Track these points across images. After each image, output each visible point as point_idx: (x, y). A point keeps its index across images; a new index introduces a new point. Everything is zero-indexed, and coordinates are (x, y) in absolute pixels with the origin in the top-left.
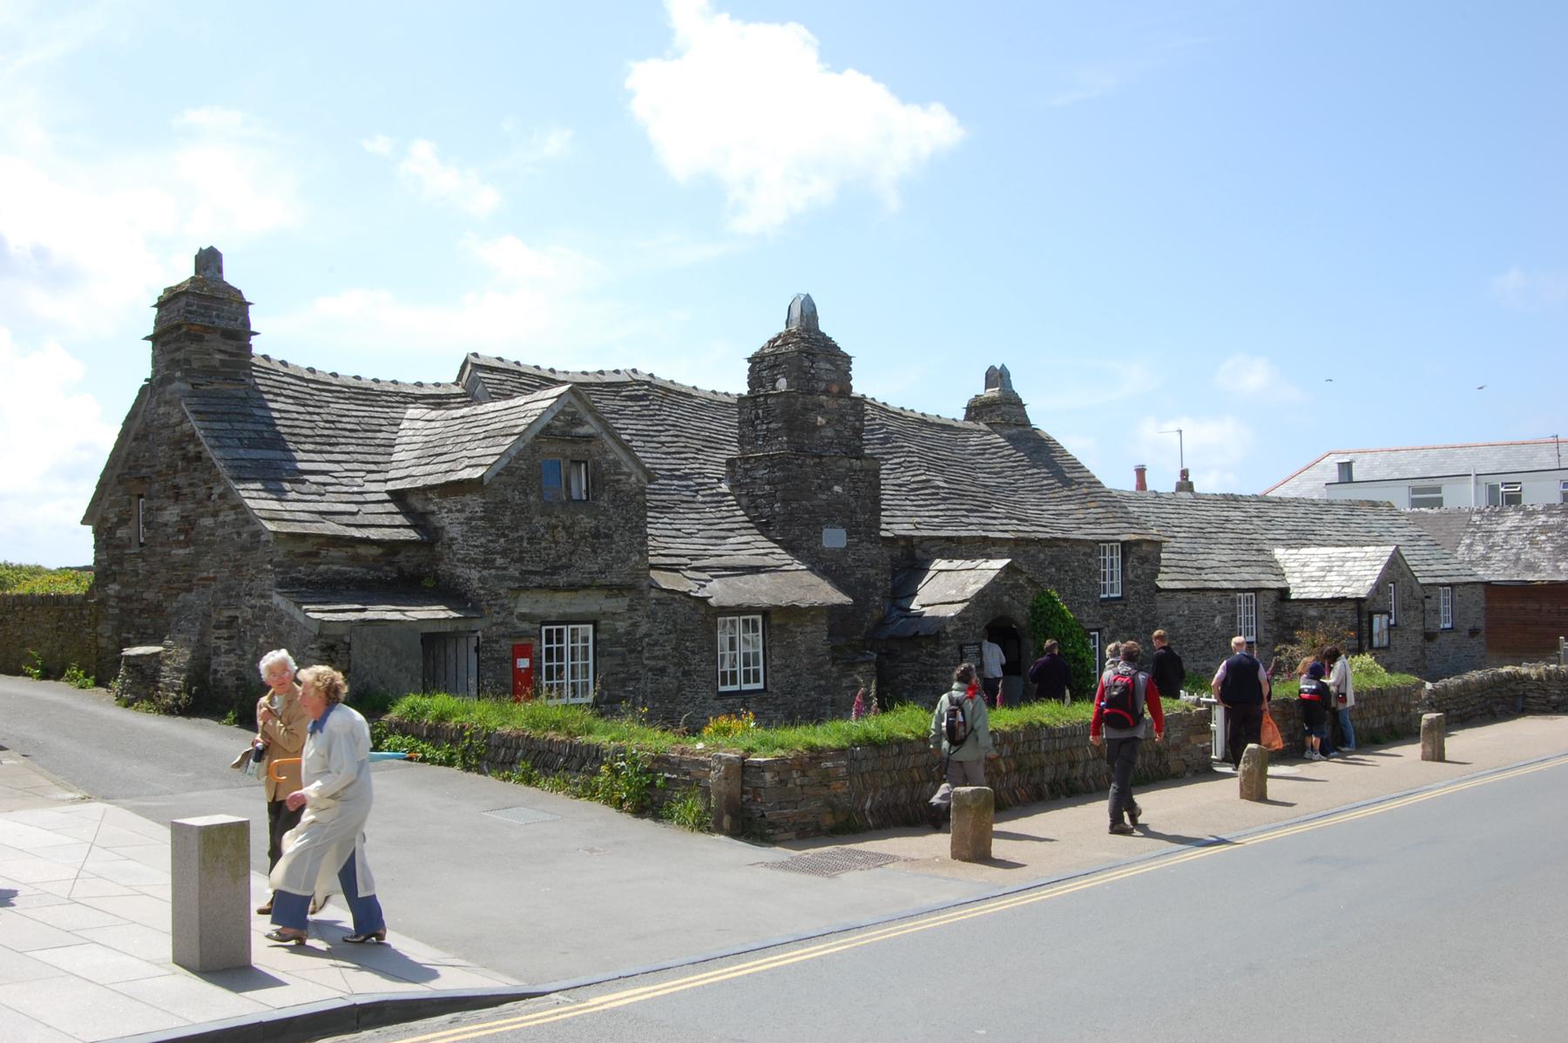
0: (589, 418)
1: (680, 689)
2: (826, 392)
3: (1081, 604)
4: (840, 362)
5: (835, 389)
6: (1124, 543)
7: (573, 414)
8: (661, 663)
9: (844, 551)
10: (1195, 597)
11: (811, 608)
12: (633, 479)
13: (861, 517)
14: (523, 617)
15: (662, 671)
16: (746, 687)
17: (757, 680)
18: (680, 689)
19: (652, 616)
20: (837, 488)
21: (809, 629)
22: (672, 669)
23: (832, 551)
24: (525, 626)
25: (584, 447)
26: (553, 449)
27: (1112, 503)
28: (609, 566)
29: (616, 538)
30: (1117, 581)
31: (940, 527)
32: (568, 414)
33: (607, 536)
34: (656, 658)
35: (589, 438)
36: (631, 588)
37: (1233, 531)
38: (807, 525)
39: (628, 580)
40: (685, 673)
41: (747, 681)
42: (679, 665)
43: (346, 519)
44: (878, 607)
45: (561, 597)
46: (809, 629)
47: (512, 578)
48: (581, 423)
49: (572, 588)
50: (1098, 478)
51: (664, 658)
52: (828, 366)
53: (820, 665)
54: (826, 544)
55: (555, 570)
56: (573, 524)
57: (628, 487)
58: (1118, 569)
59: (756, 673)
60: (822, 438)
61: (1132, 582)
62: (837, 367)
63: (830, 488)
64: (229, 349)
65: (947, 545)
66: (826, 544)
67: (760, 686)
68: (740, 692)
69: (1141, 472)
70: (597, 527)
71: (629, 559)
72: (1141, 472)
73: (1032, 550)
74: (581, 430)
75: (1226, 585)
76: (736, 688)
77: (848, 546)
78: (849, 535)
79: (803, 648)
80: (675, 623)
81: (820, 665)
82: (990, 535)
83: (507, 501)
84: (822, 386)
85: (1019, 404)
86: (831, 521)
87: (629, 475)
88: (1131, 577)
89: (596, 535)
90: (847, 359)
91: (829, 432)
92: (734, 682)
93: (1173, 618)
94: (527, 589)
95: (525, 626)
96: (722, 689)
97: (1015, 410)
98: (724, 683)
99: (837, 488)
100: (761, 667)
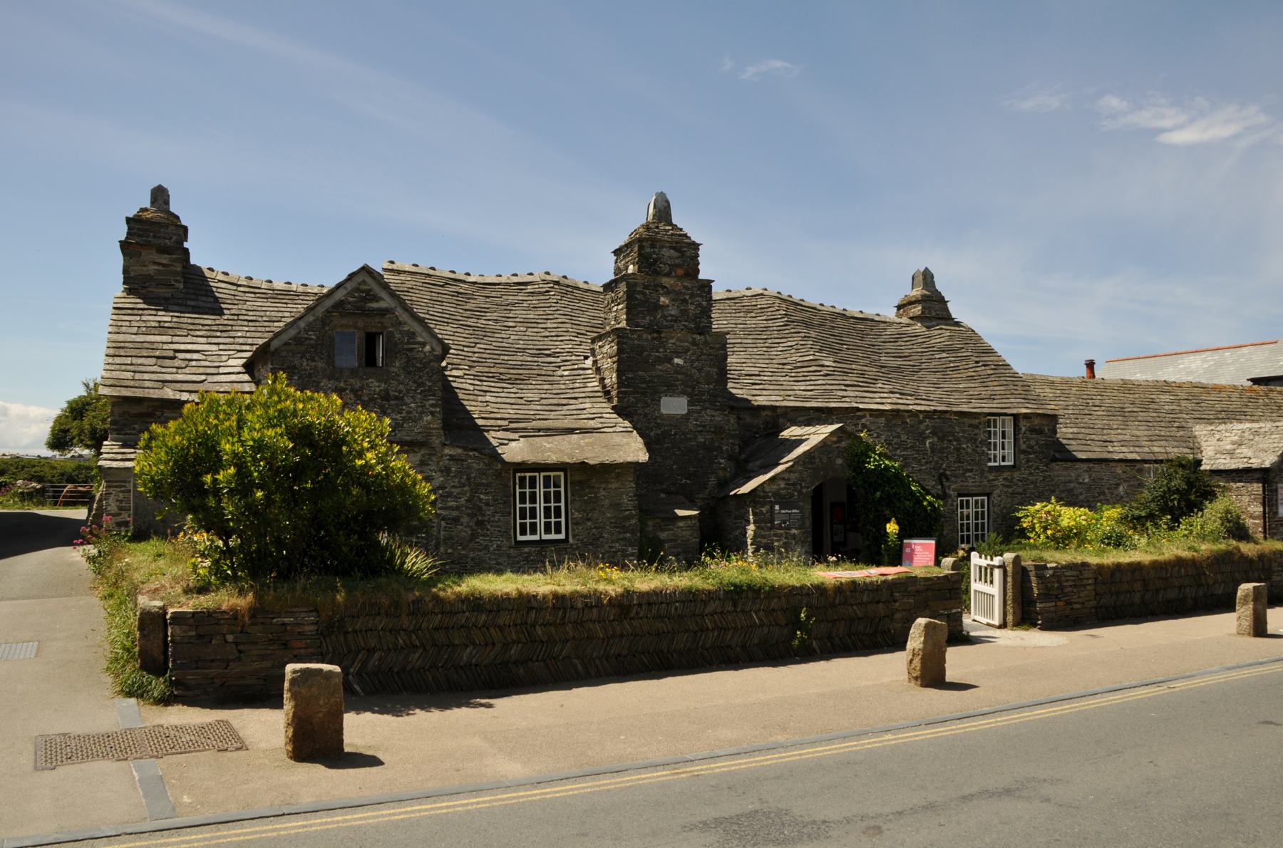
0: (383, 294)
1: (473, 537)
2: (668, 275)
4: (687, 251)
6: (1015, 416)
7: (368, 292)
8: (455, 513)
9: (686, 418)
10: (1097, 467)
11: (602, 465)
12: (428, 348)
15: (456, 520)
16: (545, 537)
17: (558, 531)
18: (473, 537)
20: (676, 360)
21: (613, 486)
22: (465, 520)
23: (671, 417)
25: (377, 319)
26: (344, 322)
27: (1022, 385)
29: (407, 400)
30: (1009, 451)
31: (806, 399)
32: (363, 291)
33: (396, 398)
34: (451, 508)
35: (384, 312)
36: (421, 445)
37: (1155, 411)
38: (644, 394)
39: (419, 438)
40: (480, 524)
41: (548, 531)
42: (472, 516)
43: (185, 386)
44: (724, 469)
46: (613, 486)
48: (376, 299)
50: (1008, 362)
51: (457, 508)
54: (664, 411)
56: (362, 388)
57: (422, 355)
58: (1009, 441)
59: (558, 525)
60: (664, 317)
61: (1024, 452)
62: (682, 253)
63: (670, 360)
64: (164, 262)
66: (664, 411)
67: (562, 536)
68: (541, 542)
69: (1090, 365)
70: (386, 391)
71: (421, 418)
72: (1090, 365)
74: (375, 305)
75: (1130, 456)
76: (536, 538)
78: (690, 403)
79: (607, 502)
80: (469, 479)
82: (861, 406)
83: (294, 367)
85: (942, 301)
86: (671, 389)
87: (424, 344)
88: (1024, 447)
89: (386, 396)
90: (696, 246)
91: (673, 311)
92: (533, 532)
96: (520, 538)
97: (937, 306)
98: (523, 532)
99: (676, 360)
100: (563, 520)
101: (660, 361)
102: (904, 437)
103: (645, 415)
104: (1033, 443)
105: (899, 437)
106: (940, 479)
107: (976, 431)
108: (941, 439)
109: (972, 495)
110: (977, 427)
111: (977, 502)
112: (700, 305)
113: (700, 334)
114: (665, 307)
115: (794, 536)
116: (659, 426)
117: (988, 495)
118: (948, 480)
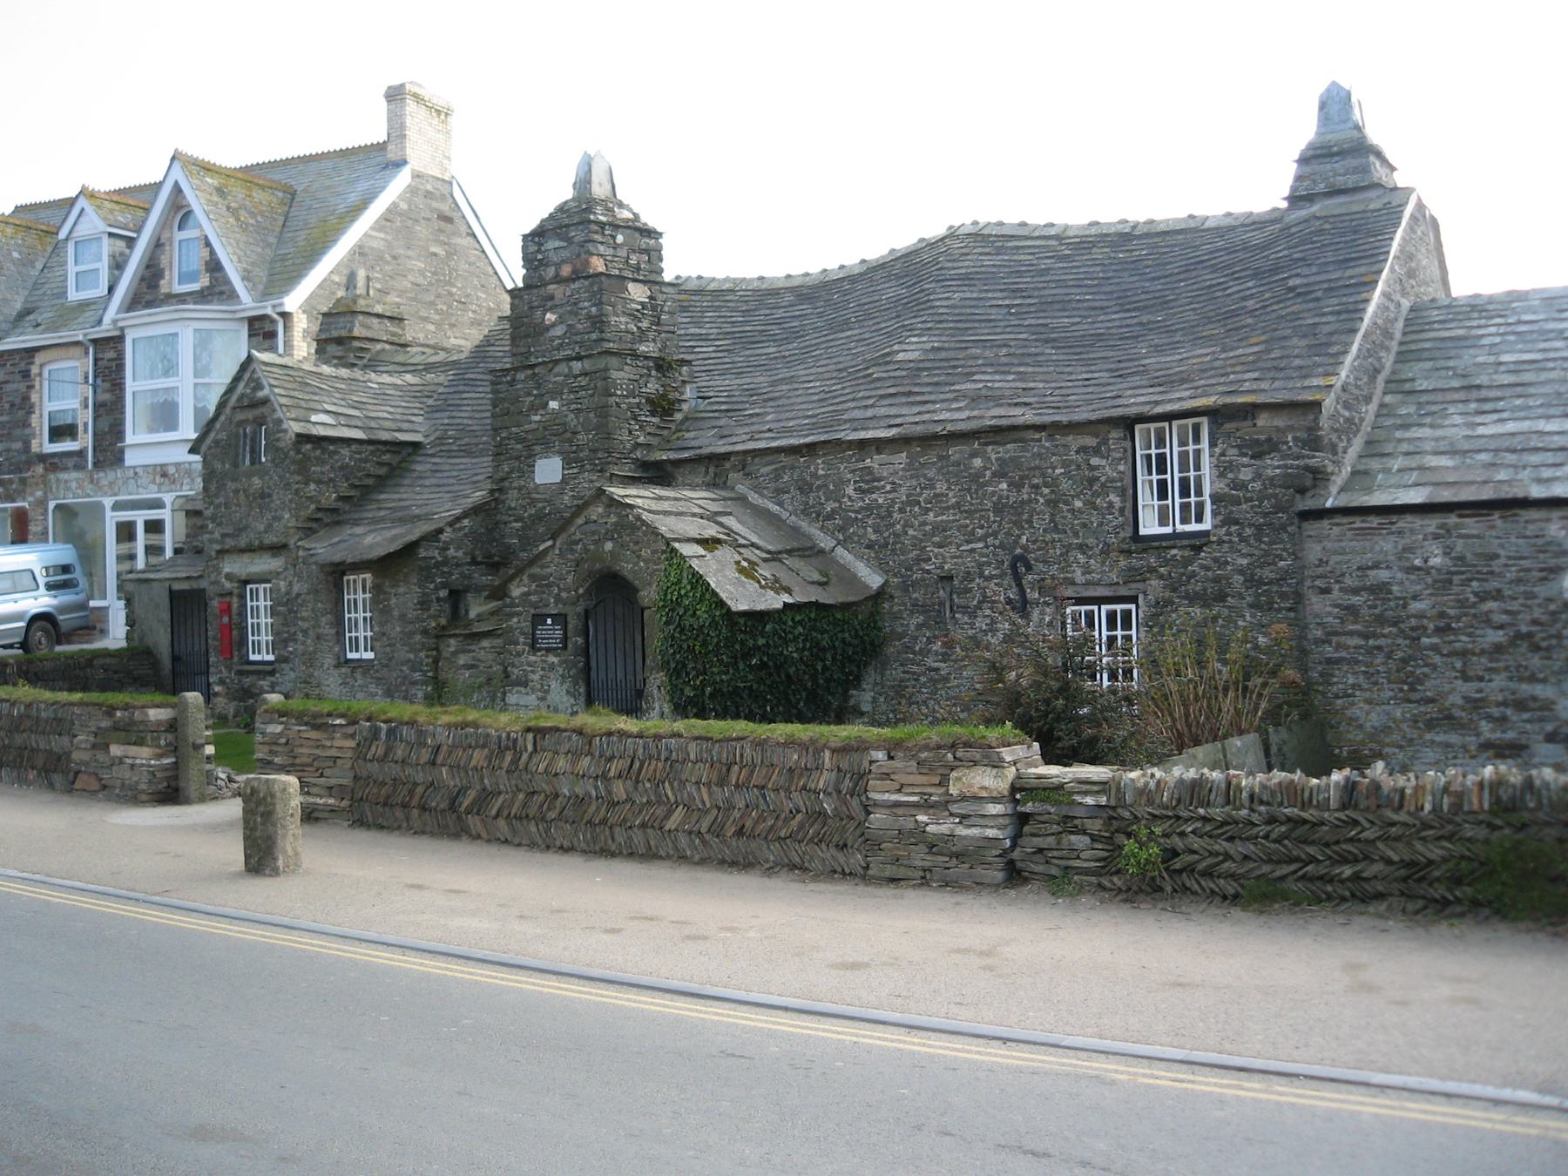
2: (558, 280)
3: (1068, 548)
5: (566, 270)
10: (1472, 525)
13: (582, 438)
14: (229, 577)
19: (300, 579)
24: (228, 585)
28: (270, 526)
38: (518, 458)
40: (318, 637)
45: (246, 558)
46: (401, 590)
47: (216, 541)
49: (249, 550)
52: (557, 244)
53: (411, 634)
54: (538, 481)
55: (240, 531)
57: (282, 444)
62: (569, 240)
65: (786, 460)
66: (538, 481)
73: (955, 452)
74: (260, 394)
77: (564, 480)
78: (567, 463)
79: (396, 613)
81: (411, 634)
84: (551, 272)
91: (559, 331)
93: (1384, 575)
94: (227, 551)
95: (228, 585)
99: (553, 405)
101: (533, 409)
102: (941, 487)
103: (520, 489)
104: (1245, 475)
105: (932, 487)
106: (1014, 567)
107: (1095, 461)
108: (1016, 486)
109: (1099, 601)
110: (1096, 451)
111: (1111, 617)
112: (589, 317)
113: (579, 358)
114: (553, 325)
115: (552, 667)
116: (533, 502)
117: (1134, 599)
118: (1029, 568)
